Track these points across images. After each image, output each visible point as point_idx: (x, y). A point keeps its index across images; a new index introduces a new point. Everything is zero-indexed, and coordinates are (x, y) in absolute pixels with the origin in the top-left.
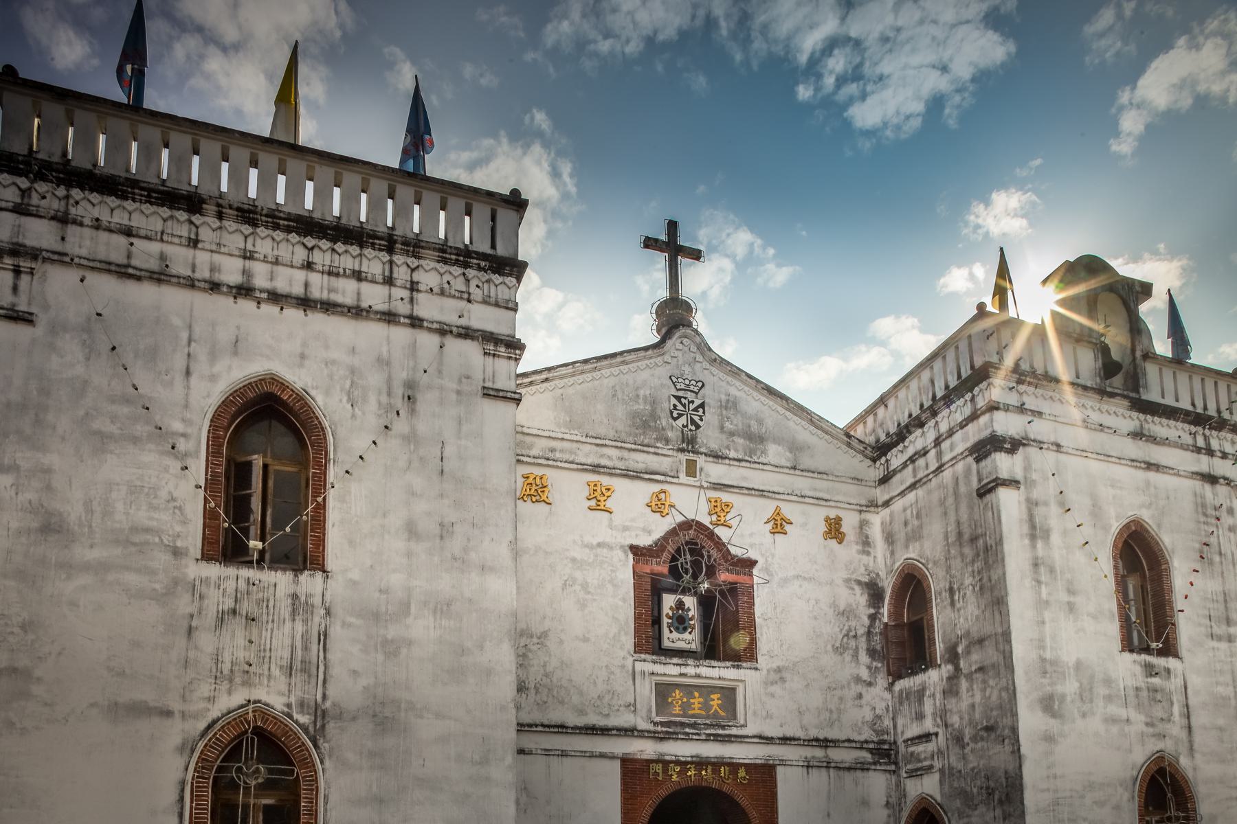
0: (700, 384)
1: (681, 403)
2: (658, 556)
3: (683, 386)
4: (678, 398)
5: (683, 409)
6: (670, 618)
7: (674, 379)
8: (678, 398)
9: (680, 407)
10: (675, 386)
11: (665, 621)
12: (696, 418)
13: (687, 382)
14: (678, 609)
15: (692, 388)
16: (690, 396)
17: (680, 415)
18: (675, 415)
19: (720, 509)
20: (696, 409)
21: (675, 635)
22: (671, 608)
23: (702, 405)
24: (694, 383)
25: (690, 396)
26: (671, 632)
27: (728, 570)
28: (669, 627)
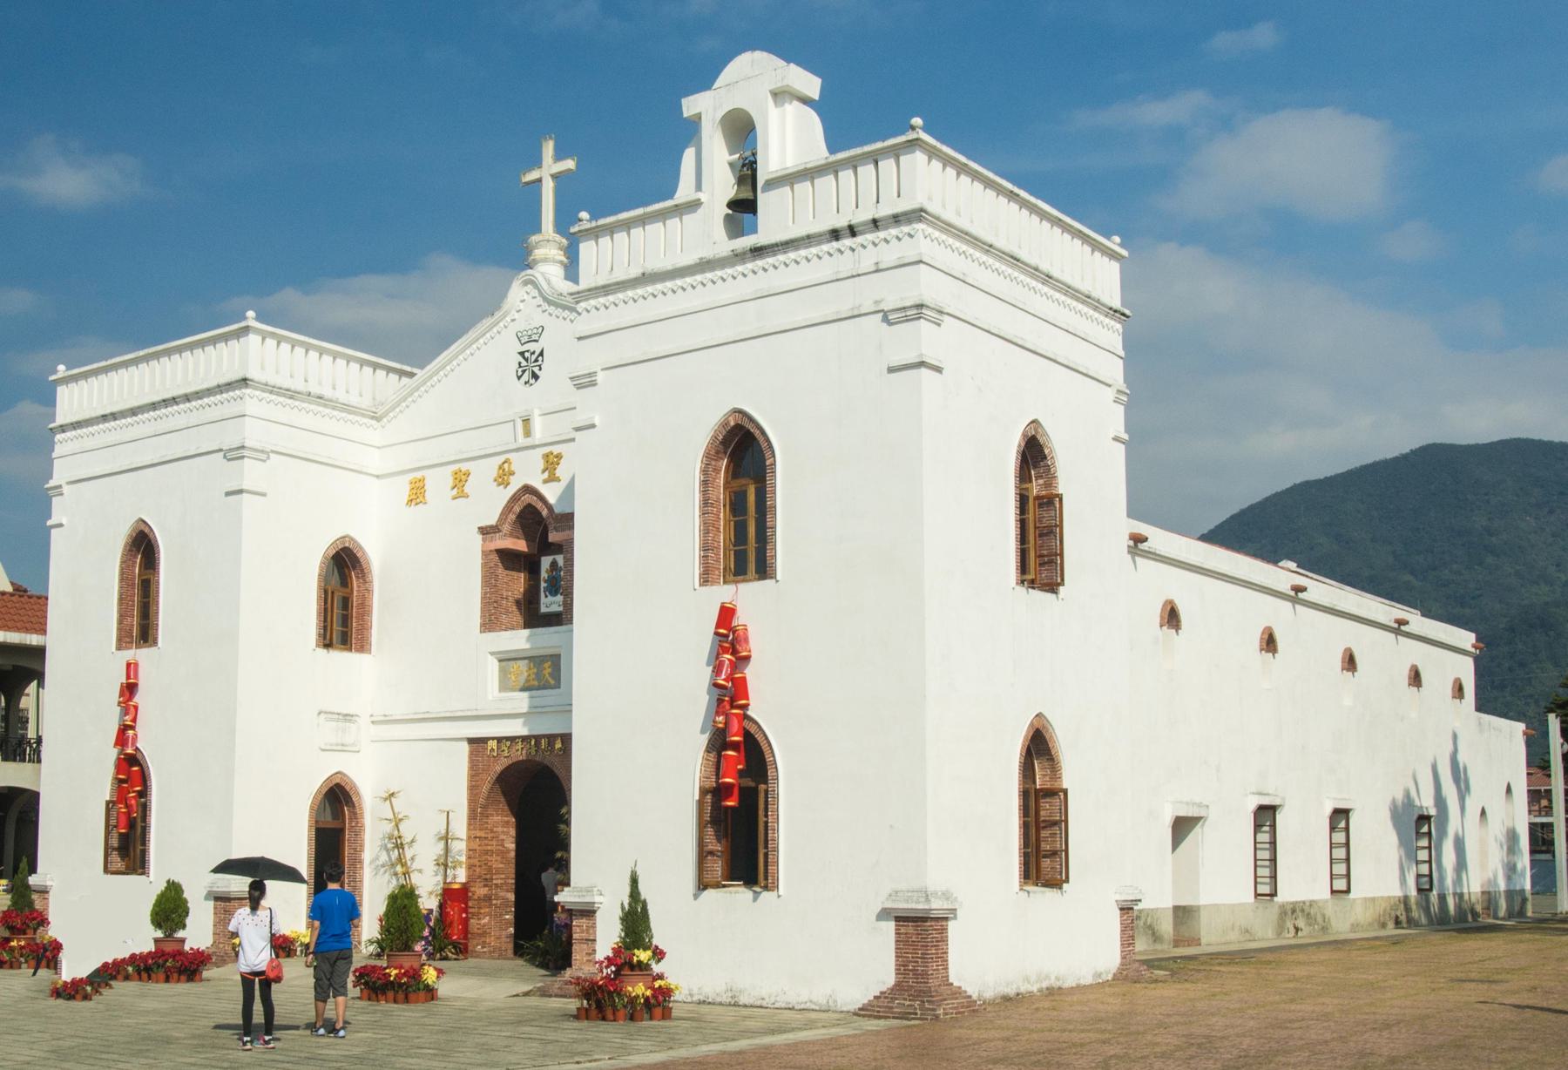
0: (541, 329)
1: (524, 358)
2: (500, 531)
3: (526, 339)
4: (522, 354)
5: (533, 360)
6: (545, 581)
7: (520, 335)
8: (522, 354)
9: (524, 363)
10: (520, 341)
11: (543, 585)
12: (536, 370)
13: (530, 333)
14: (552, 571)
15: (533, 338)
16: (531, 346)
17: (524, 372)
18: (520, 374)
19: (551, 464)
20: (536, 361)
21: (550, 598)
22: (547, 572)
23: (541, 354)
24: (535, 331)
25: (531, 346)
26: (546, 596)
27: (556, 529)
28: (544, 592)
